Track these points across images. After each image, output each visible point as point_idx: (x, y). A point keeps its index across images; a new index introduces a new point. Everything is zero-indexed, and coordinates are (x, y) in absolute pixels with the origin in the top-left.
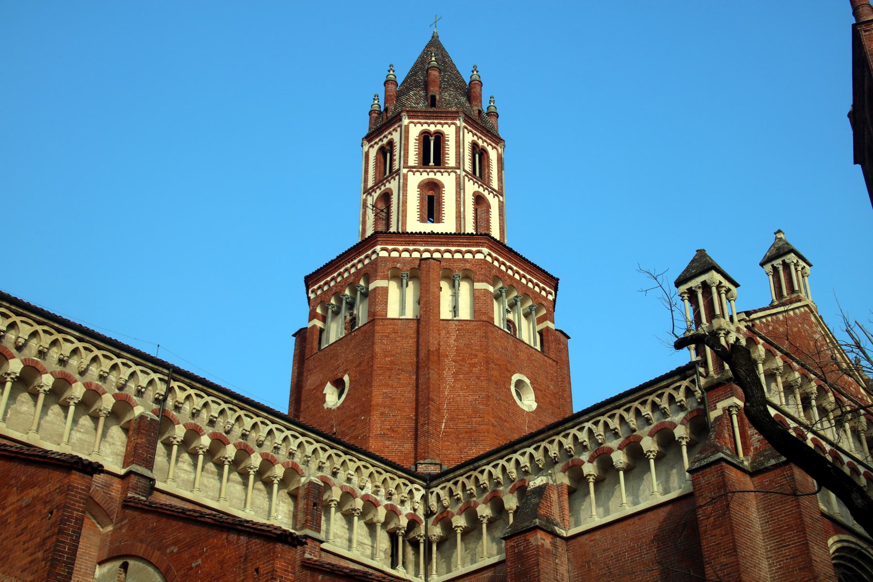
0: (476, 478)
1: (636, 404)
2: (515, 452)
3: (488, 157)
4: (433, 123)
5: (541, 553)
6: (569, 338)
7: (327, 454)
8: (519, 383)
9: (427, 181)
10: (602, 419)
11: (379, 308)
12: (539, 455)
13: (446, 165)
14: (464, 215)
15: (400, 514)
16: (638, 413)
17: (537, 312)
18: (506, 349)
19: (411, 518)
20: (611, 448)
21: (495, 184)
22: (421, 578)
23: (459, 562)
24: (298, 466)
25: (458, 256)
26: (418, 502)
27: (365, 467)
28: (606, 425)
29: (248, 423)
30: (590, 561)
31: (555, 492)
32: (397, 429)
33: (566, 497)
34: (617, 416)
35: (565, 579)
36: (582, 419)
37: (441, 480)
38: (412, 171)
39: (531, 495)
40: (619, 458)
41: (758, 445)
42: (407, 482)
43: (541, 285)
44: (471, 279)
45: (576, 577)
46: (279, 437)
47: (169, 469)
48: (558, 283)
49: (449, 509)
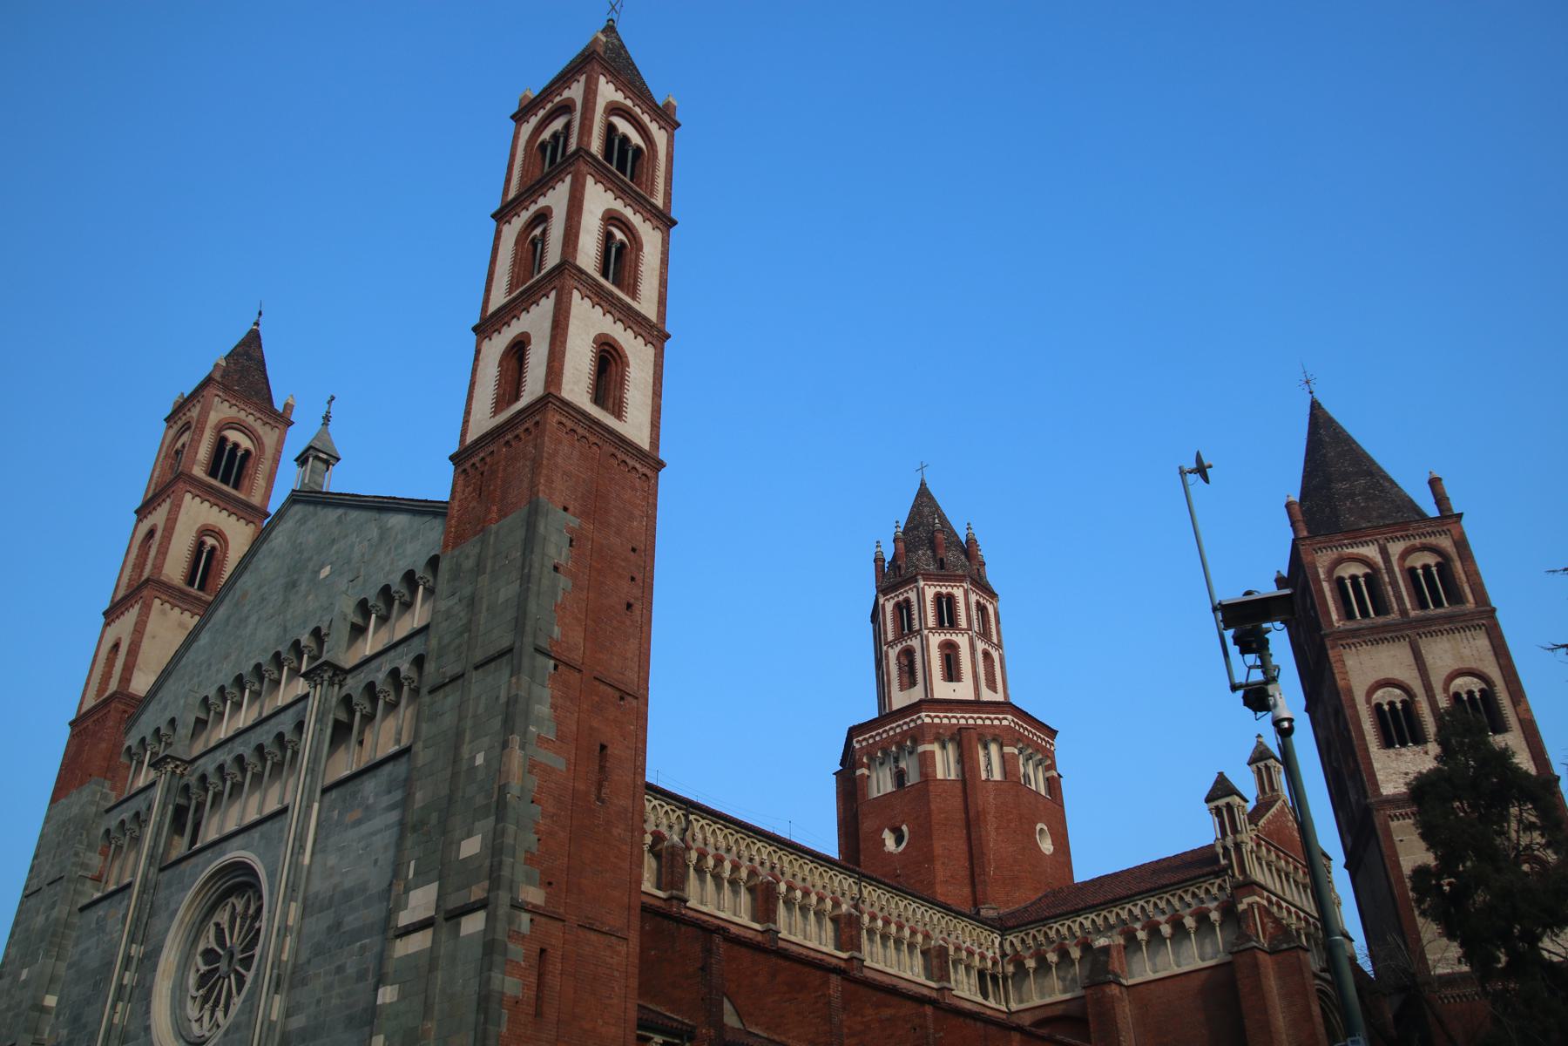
1: (1180, 892)
2: (1079, 916)
3: (988, 613)
4: (944, 585)
8: (1041, 830)
10: (1153, 900)
11: (930, 770)
12: (1099, 921)
16: (1181, 898)
25: (988, 722)
28: (1155, 905)
36: (1136, 898)
40: (1166, 930)
41: (1272, 930)
47: (972, 1001)
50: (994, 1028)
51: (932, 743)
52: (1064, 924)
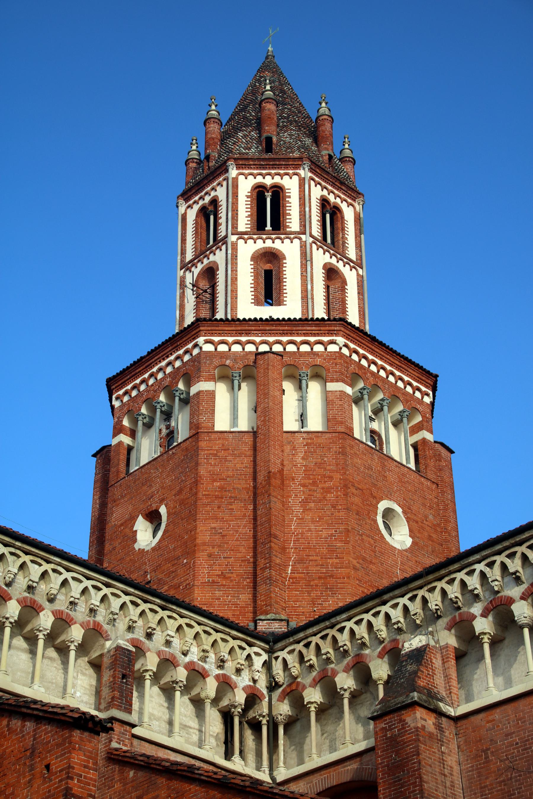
0: (334, 637)
2: (384, 603)
3: (343, 218)
4: (269, 174)
5: (421, 738)
6: (452, 452)
7: (139, 610)
8: (388, 512)
9: (263, 251)
10: (499, 559)
11: (203, 418)
12: (415, 607)
13: (288, 230)
14: (312, 295)
15: (236, 687)
17: (410, 418)
18: (370, 468)
19: (249, 692)
20: (511, 598)
21: (352, 253)
22: (264, 772)
23: (314, 750)
24: (102, 626)
25: (305, 348)
26: (258, 671)
27: (189, 625)
28: (504, 567)
29: (35, 571)
30: (488, 749)
31: (439, 656)
32: (230, 575)
33: (453, 662)
34: (518, 555)
35: (455, 773)
36: (471, 559)
37: (287, 641)
38: (243, 239)
39: (406, 661)
42: (244, 645)
43: (415, 384)
44: (323, 378)
45: (470, 771)
46: (76, 589)
48: (436, 381)
49: (299, 680)
50: (49, 728)
51: (211, 378)
52: (362, 620)
